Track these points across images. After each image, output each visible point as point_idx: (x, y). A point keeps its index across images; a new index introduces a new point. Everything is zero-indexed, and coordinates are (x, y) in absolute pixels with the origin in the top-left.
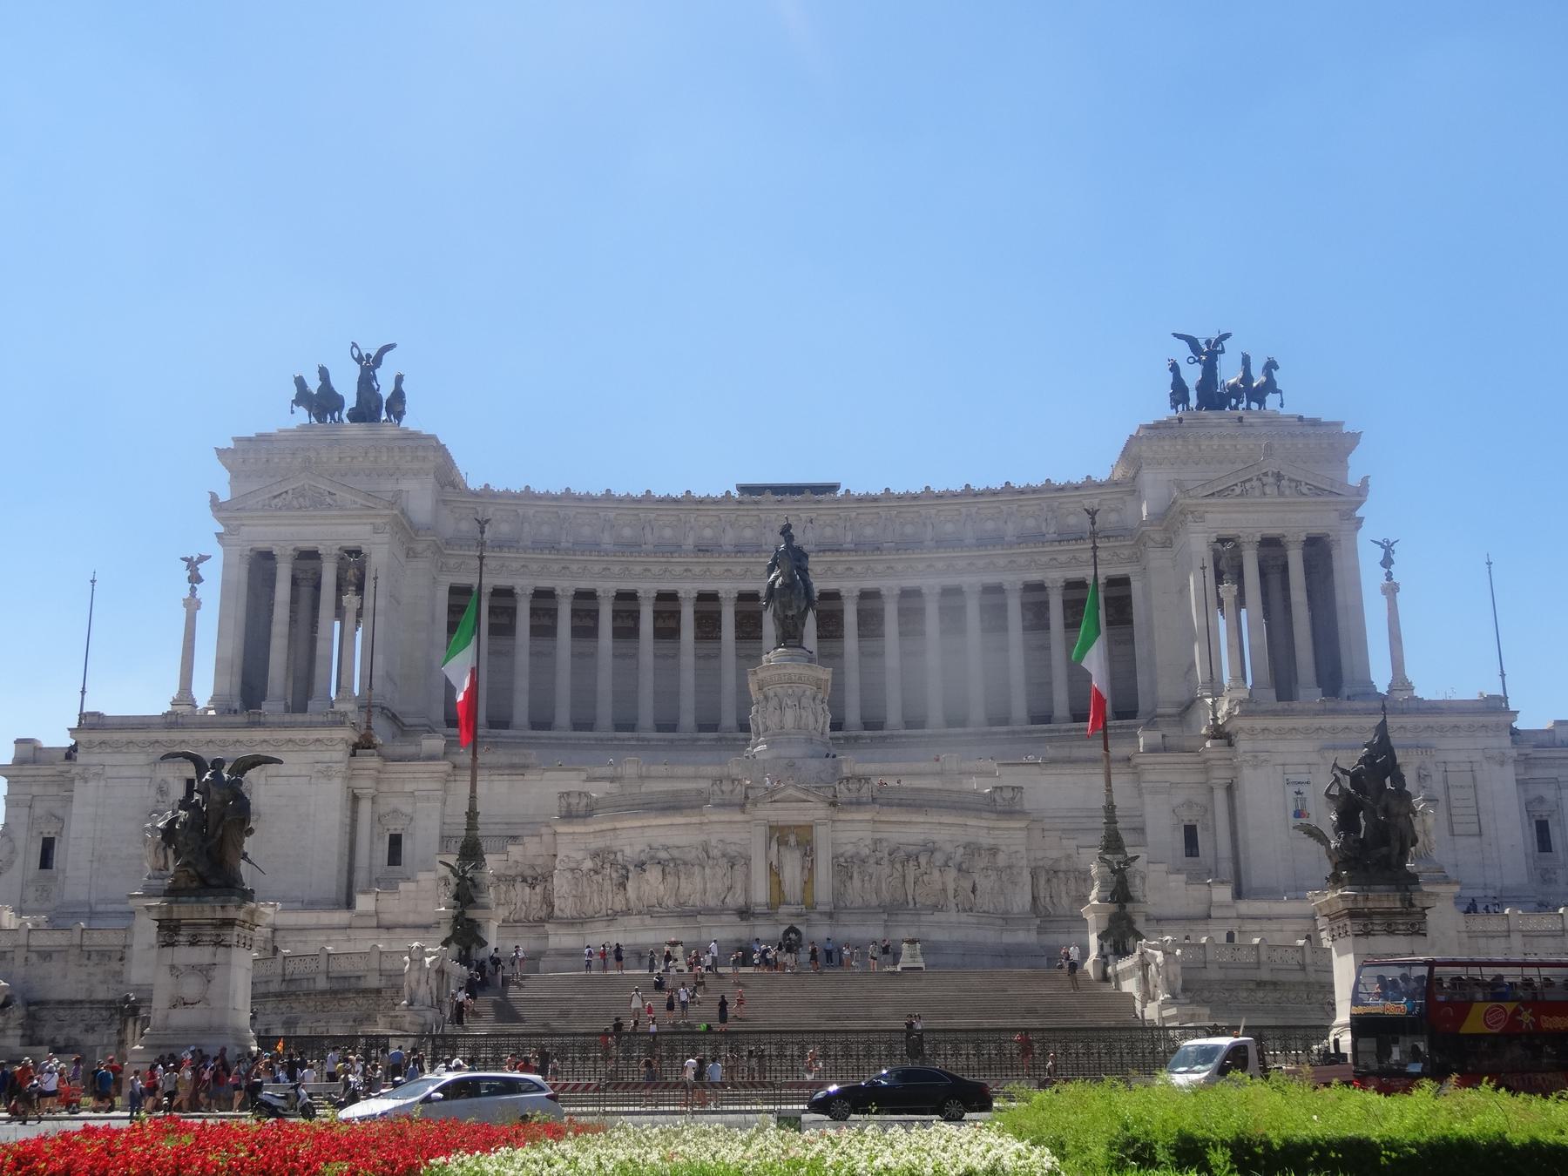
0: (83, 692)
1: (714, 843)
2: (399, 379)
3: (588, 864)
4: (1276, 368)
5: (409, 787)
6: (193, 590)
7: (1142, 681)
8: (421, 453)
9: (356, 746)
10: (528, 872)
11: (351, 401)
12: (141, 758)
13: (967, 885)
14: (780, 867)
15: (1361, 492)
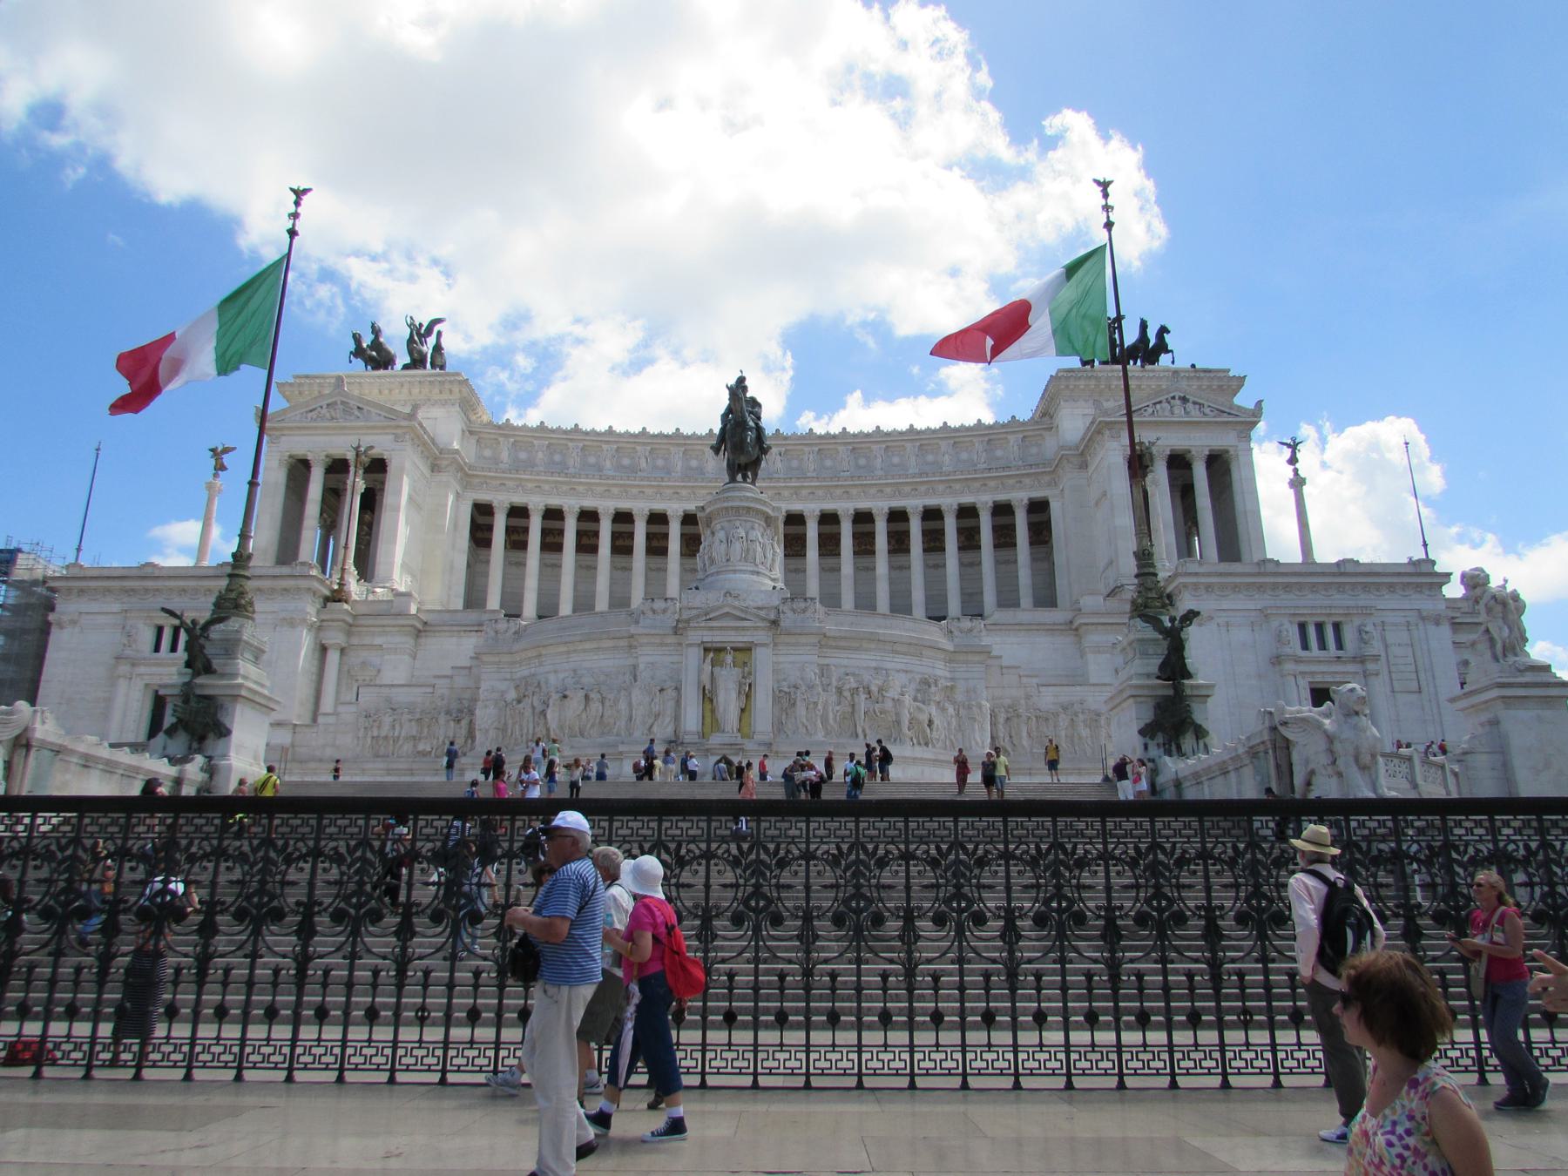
0: (79, 549)
1: (642, 667)
2: (439, 334)
3: (512, 695)
4: (1168, 332)
5: (378, 641)
6: (216, 476)
7: (1061, 583)
8: (447, 386)
9: (327, 600)
10: (454, 706)
11: (403, 359)
12: (116, 607)
13: (924, 718)
14: (714, 690)
15: (1257, 412)
